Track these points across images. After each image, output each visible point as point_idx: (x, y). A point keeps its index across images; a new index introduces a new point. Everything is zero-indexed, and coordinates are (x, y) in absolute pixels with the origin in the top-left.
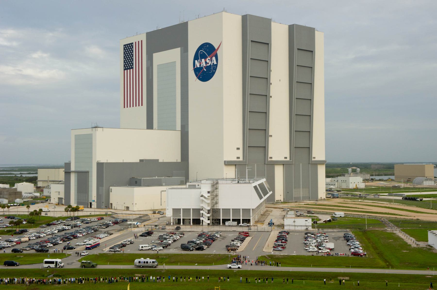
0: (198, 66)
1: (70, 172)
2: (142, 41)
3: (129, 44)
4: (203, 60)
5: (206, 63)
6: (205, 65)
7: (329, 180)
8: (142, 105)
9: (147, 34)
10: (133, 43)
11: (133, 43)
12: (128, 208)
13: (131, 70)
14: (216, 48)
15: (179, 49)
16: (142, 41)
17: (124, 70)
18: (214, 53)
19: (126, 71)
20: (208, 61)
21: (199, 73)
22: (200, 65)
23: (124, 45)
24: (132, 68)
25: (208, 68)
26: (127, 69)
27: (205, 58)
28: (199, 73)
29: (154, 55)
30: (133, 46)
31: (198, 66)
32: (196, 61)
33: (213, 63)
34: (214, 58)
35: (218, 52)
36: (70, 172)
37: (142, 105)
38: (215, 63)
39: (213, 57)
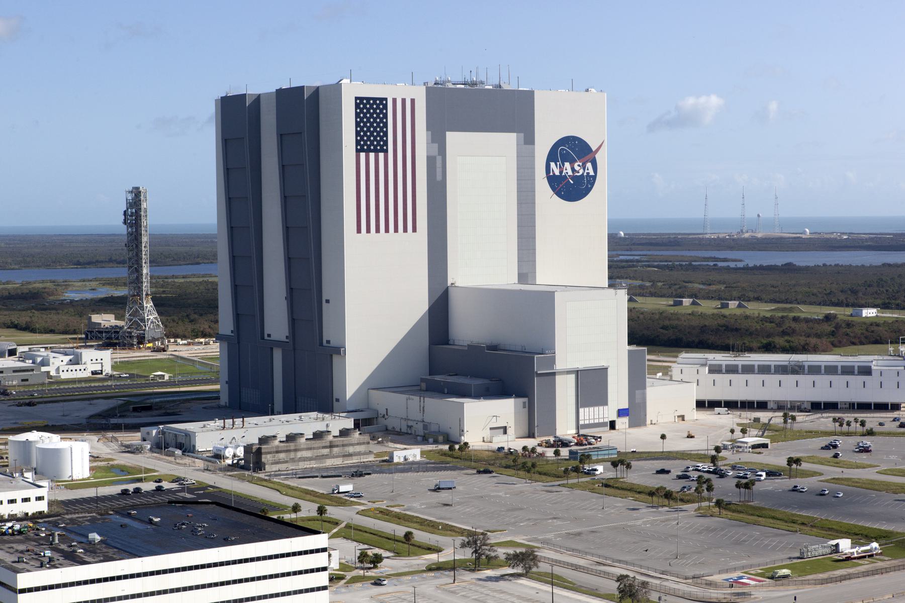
0: (557, 173)
1: (554, 374)
2: (413, 101)
3: (375, 99)
4: (567, 165)
5: (573, 170)
6: (570, 173)
7: (634, 348)
8: (414, 230)
9: (429, 91)
10: (386, 99)
11: (386, 99)
12: (682, 418)
13: (381, 155)
14: (594, 149)
15: (515, 135)
16: (413, 101)
17: (358, 151)
18: (589, 156)
19: (363, 155)
20: (577, 168)
21: (558, 185)
22: (561, 172)
23: (356, 98)
24: (386, 151)
25: (578, 179)
26: (368, 151)
27: (572, 162)
28: (558, 185)
29: (449, 134)
30: (385, 107)
31: (557, 173)
32: (553, 165)
33: (588, 173)
34: (589, 165)
35: (597, 156)
36: (554, 374)
37: (414, 230)
38: (592, 173)
39: (587, 162)
